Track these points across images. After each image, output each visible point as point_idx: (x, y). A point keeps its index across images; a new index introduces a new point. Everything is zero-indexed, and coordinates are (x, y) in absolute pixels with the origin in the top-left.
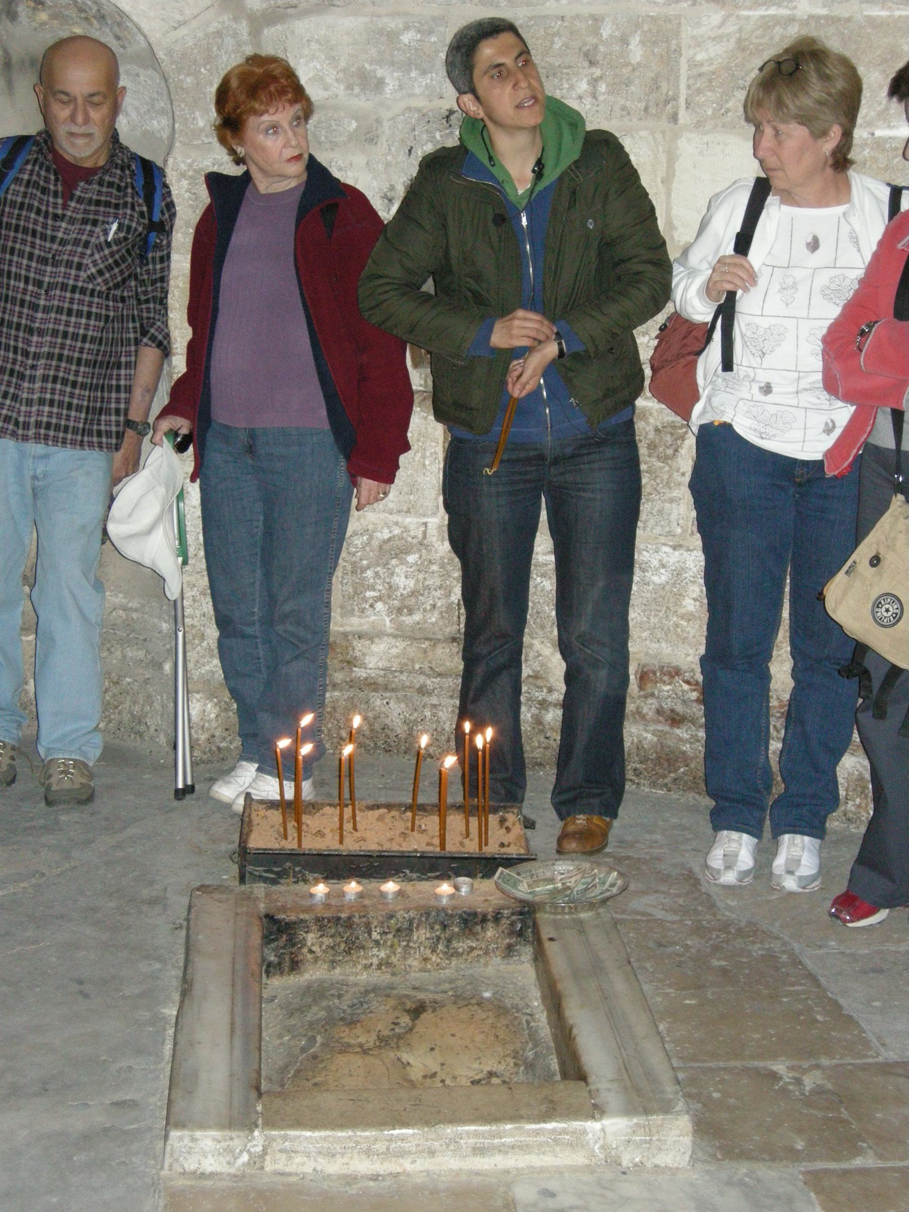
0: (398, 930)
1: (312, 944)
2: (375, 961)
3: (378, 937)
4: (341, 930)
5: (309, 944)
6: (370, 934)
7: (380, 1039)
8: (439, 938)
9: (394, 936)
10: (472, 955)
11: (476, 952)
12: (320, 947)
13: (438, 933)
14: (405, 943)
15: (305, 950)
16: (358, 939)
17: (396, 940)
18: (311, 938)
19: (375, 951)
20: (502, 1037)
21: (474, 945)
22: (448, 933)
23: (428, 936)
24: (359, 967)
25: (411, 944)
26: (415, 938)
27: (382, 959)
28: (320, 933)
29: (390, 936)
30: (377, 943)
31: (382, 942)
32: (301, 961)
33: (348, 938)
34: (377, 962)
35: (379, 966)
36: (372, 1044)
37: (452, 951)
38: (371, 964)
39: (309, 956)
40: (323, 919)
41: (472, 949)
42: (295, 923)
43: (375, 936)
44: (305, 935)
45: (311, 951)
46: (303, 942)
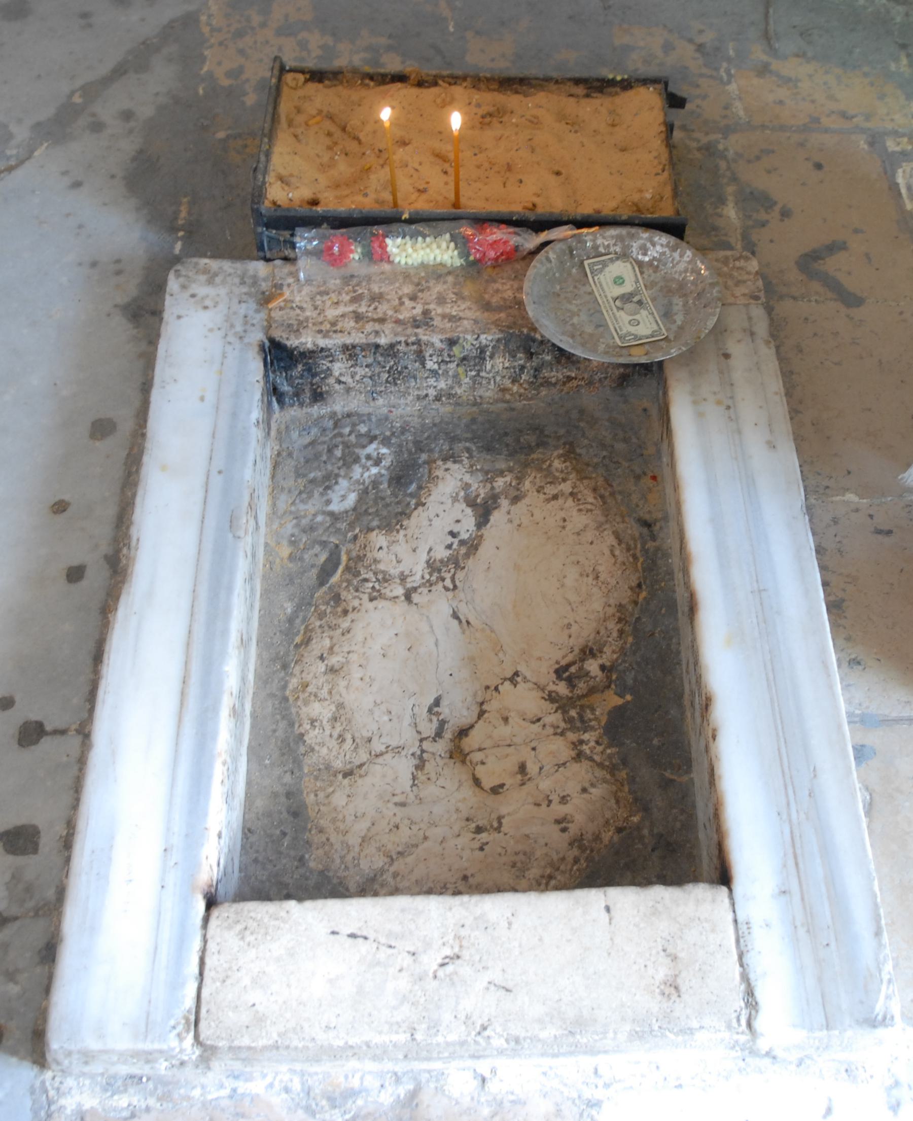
0: (464, 359)
1: (341, 374)
2: (432, 393)
3: (436, 367)
4: (380, 359)
5: (337, 374)
6: (423, 364)
7: (433, 566)
8: (522, 368)
9: (458, 365)
10: (570, 385)
11: (575, 383)
12: (352, 377)
13: (521, 362)
14: (473, 373)
15: (331, 381)
16: (406, 368)
17: (461, 370)
18: (338, 368)
19: (432, 381)
20: (603, 577)
21: (573, 375)
22: (535, 362)
23: (507, 365)
24: (410, 398)
25: (483, 374)
26: (489, 367)
27: (442, 389)
28: (350, 363)
29: (452, 366)
30: (434, 373)
31: (440, 372)
32: (327, 392)
33: (391, 368)
34: (435, 393)
35: (438, 398)
36: (418, 577)
37: (540, 381)
38: (427, 395)
39: (337, 387)
40: (354, 347)
41: (570, 379)
42: (313, 352)
43: (430, 365)
44: (329, 365)
45: (339, 382)
46: (329, 372)
